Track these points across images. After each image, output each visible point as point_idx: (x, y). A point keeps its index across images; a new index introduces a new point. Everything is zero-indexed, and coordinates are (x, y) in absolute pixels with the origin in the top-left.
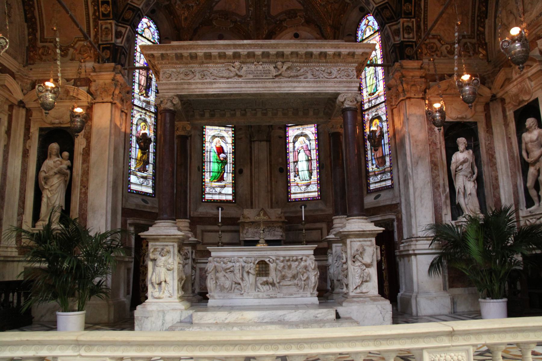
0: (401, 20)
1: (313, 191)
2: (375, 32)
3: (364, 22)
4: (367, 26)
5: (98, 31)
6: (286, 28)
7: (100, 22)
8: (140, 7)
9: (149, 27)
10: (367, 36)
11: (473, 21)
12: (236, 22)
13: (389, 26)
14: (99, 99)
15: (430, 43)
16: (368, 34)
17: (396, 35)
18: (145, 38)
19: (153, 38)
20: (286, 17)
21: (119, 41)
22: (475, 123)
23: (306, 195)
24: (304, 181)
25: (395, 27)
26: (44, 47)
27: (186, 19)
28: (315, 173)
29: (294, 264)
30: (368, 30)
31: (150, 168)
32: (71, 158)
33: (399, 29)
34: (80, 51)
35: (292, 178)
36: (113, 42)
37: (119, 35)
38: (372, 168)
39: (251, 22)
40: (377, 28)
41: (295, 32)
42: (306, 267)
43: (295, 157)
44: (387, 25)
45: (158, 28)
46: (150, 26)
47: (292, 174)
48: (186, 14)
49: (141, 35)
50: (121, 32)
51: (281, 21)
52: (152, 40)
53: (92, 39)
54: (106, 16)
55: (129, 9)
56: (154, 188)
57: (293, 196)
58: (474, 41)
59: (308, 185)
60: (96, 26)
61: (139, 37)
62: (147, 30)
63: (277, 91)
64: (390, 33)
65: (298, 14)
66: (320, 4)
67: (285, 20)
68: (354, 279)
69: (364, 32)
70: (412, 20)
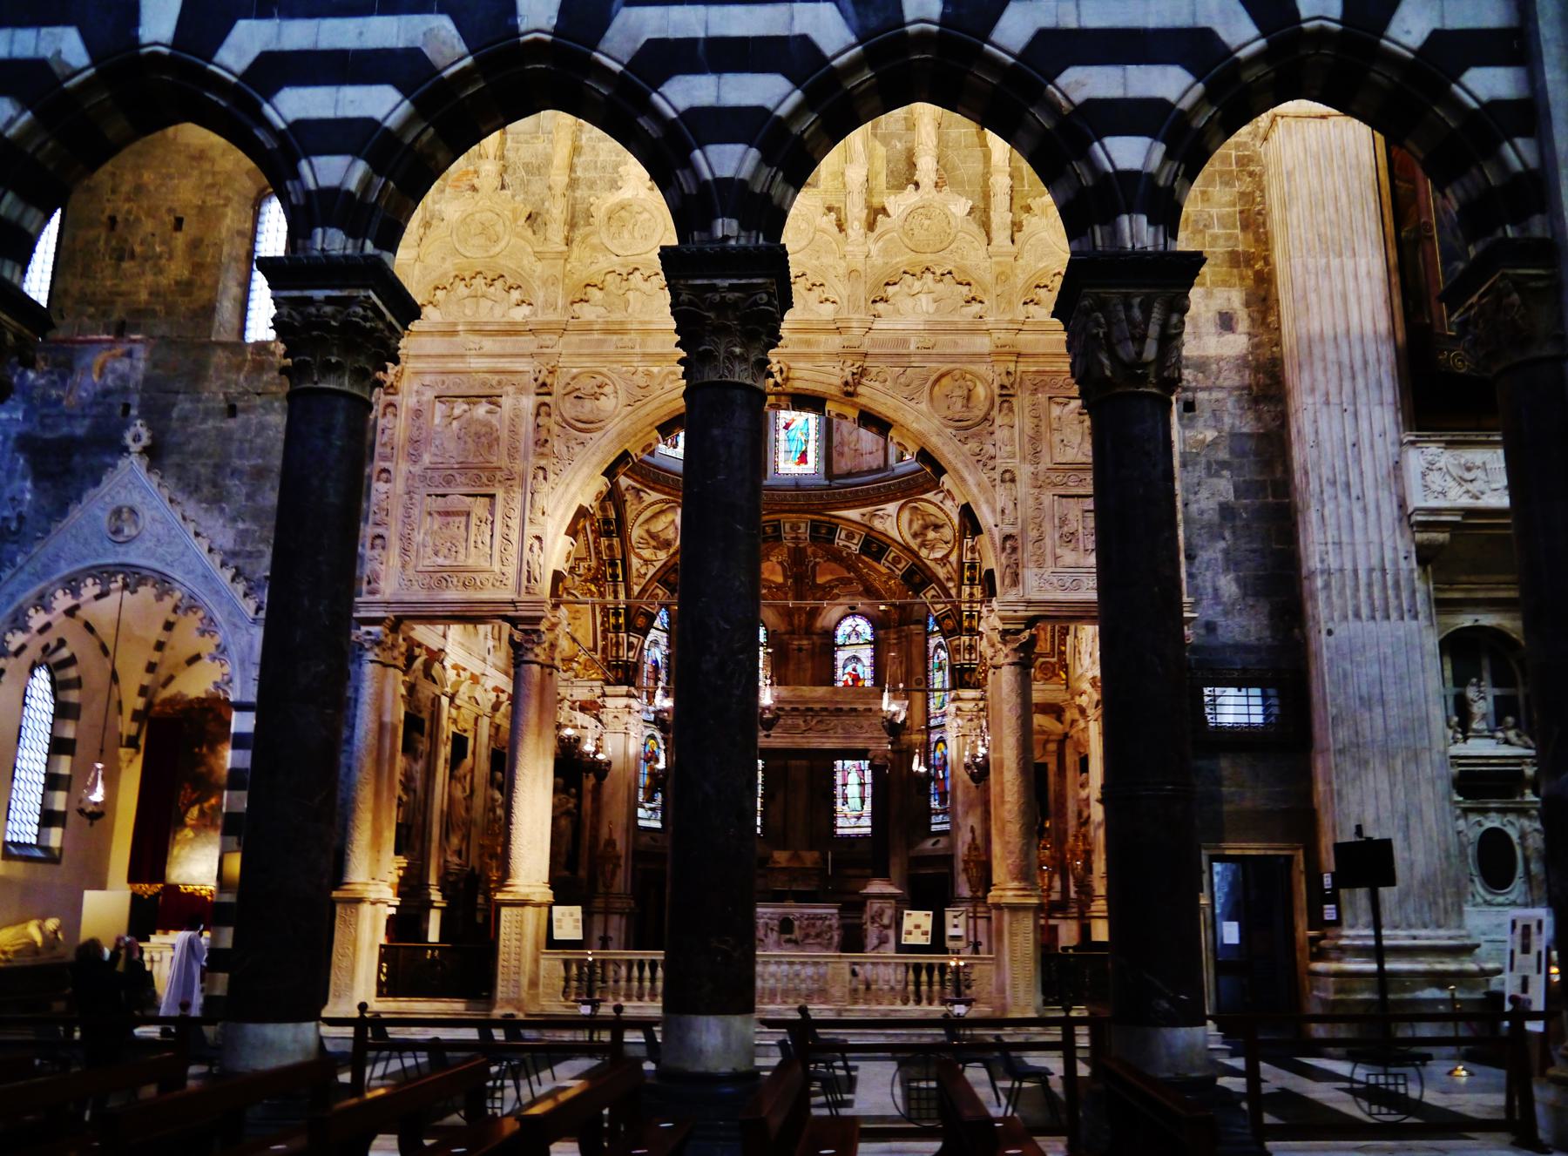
1: (865, 827)
6: (838, 596)
11: (1053, 637)
14: (611, 728)
22: (1045, 765)
23: (856, 831)
24: (853, 811)
28: (868, 802)
29: (819, 923)
31: (659, 797)
32: (579, 797)
35: (839, 807)
38: (935, 804)
42: (830, 926)
43: (844, 778)
47: (840, 801)
51: (832, 588)
56: (662, 821)
57: (839, 831)
58: (1054, 660)
59: (859, 818)
60: (605, 638)
63: (806, 746)
68: (872, 940)
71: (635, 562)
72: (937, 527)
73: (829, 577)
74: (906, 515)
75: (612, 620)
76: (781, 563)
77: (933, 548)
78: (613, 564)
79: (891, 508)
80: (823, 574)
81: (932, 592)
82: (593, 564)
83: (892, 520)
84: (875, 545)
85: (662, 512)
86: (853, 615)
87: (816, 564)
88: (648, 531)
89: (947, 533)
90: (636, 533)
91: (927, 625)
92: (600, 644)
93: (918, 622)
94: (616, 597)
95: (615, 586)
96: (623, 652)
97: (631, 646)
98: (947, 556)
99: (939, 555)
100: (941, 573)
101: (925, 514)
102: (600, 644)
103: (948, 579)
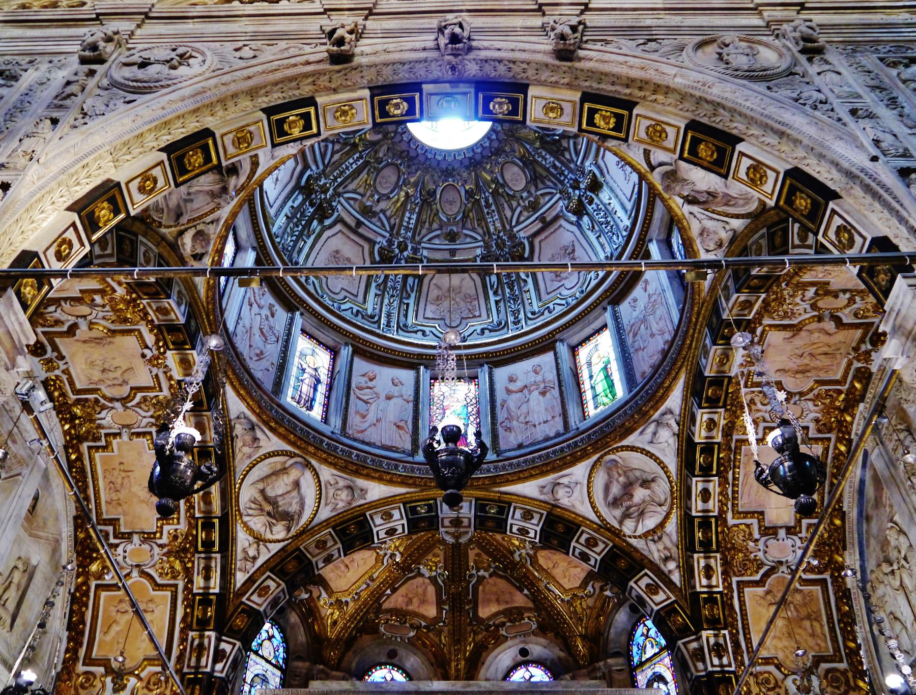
0: (704, 634)
2: (662, 650)
3: (641, 630)
4: (647, 637)
5: (185, 648)
7: (191, 634)
8: (262, 609)
9: (270, 638)
10: (648, 655)
12: (418, 628)
13: (685, 644)
15: (761, 673)
16: (650, 652)
17: (698, 660)
18: (262, 657)
19: (276, 657)
20: (503, 620)
21: (219, 666)
25: (695, 645)
26: (86, 673)
27: (335, 623)
30: (649, 646)
33: (701, 649)
34: (149, 682)
36: (208, 669)
37: (219, 655)
39: (446, 629)
40: (663, 642)
41: (521, 646)
44: (680, 643)
45: (285, 639)
46: (273, 636)
48: (335, 617)
49: (256, 653)
50: (224, 651)
52: (274, 661)
53: (171, 664)
54: (203, 625)
55: (243, 611)
60: (183, 640)
61: (253, 656)
62: (266, 643)
64: (687, 657)
65: (526, 615)
66: (562, 600)
67: (503, 624)
69: (643, 649)
70: (723, 632)
71: (242, 538)
72: (646, 484)
73: (494, 608)
74: (600, 479)
75: (198, 613)
76: (433, 580)
77: (642, 514)
78: (208, 526)
79: (580, 471)
80: (488, 602)
81: (645, 581)
82: (183, 527)
83: (578, 489)
84: (559, 529)
85: (284, 470)
86: (526, 664)
87: (481, 579)
88: (262, 492)
89: (662, 489)
90: (247, 494)
91: (629, 657)
92: (175, 653)
93: (617, 655)
94: (207, 578)
95: (208, 559)
96: (206, 662)
97: (219, 655)
98: (662, 525)
99: (650, 523)
100: (655, 552)
101: (627, 471)
102: (175, 653)
103: (666, 559)
